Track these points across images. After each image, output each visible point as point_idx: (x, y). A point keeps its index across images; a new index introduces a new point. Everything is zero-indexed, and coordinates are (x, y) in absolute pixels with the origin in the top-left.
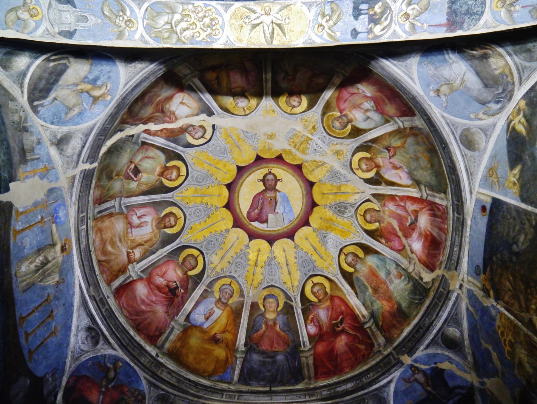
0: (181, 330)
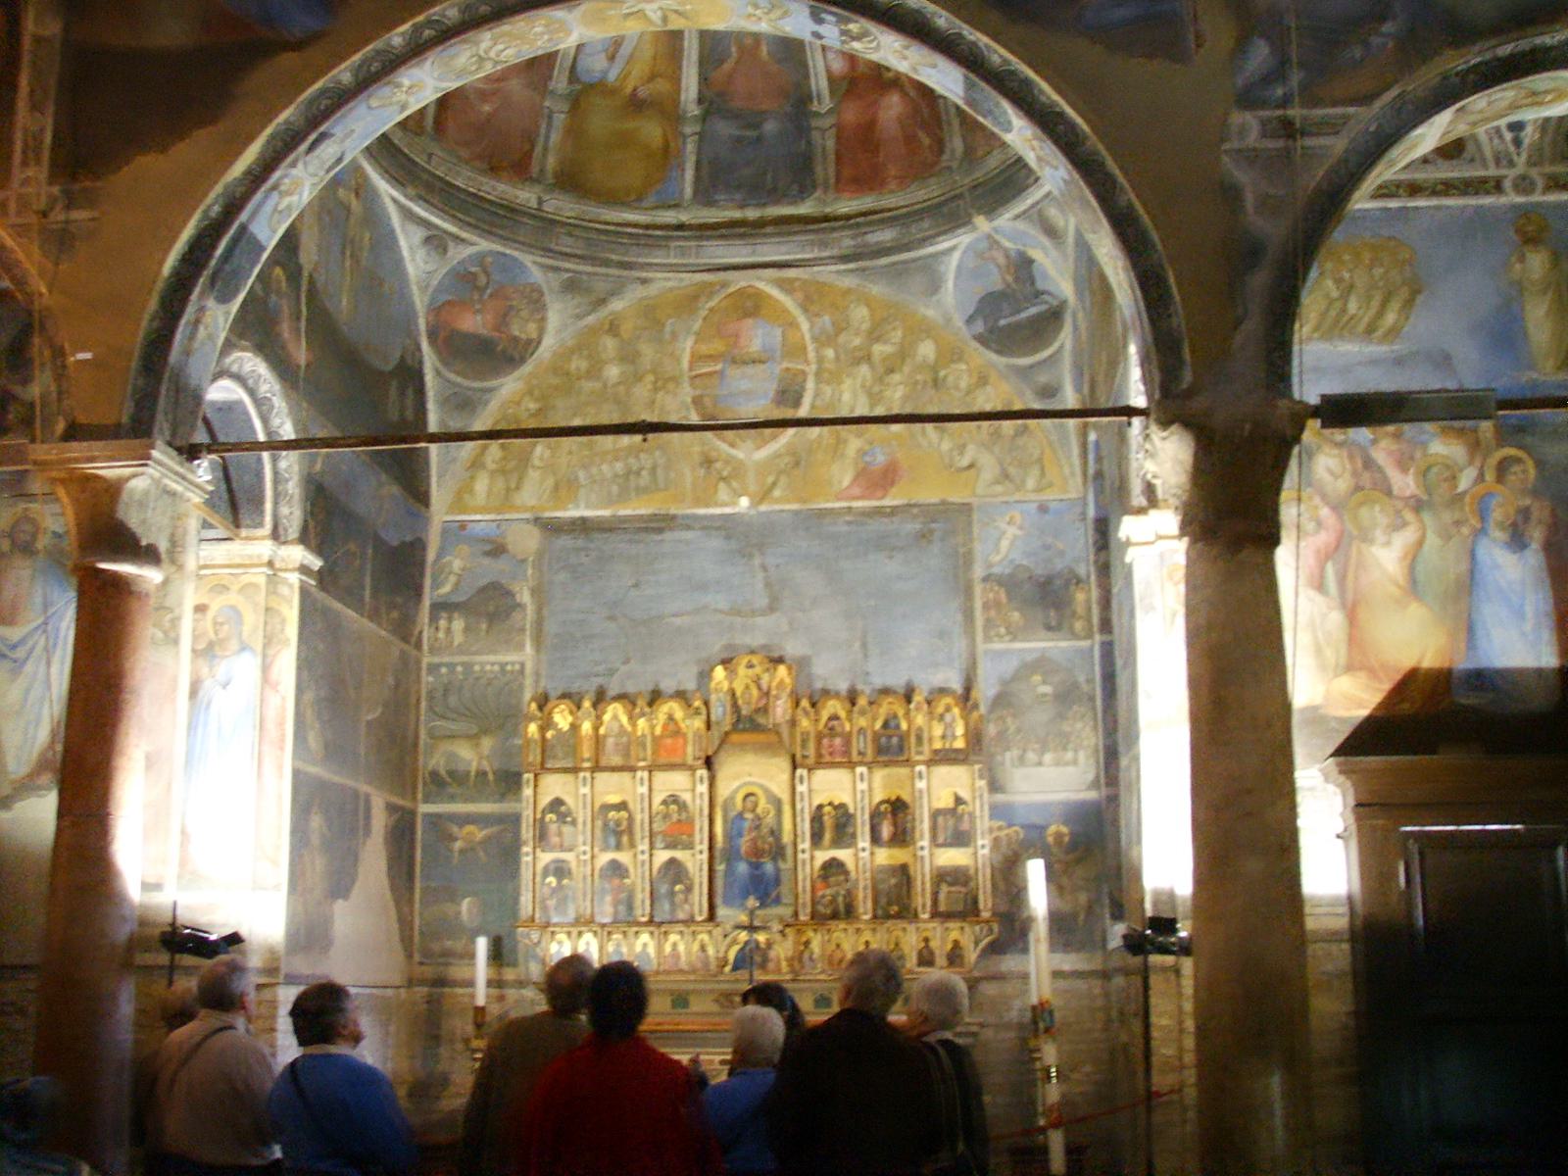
0: (566, 107)
